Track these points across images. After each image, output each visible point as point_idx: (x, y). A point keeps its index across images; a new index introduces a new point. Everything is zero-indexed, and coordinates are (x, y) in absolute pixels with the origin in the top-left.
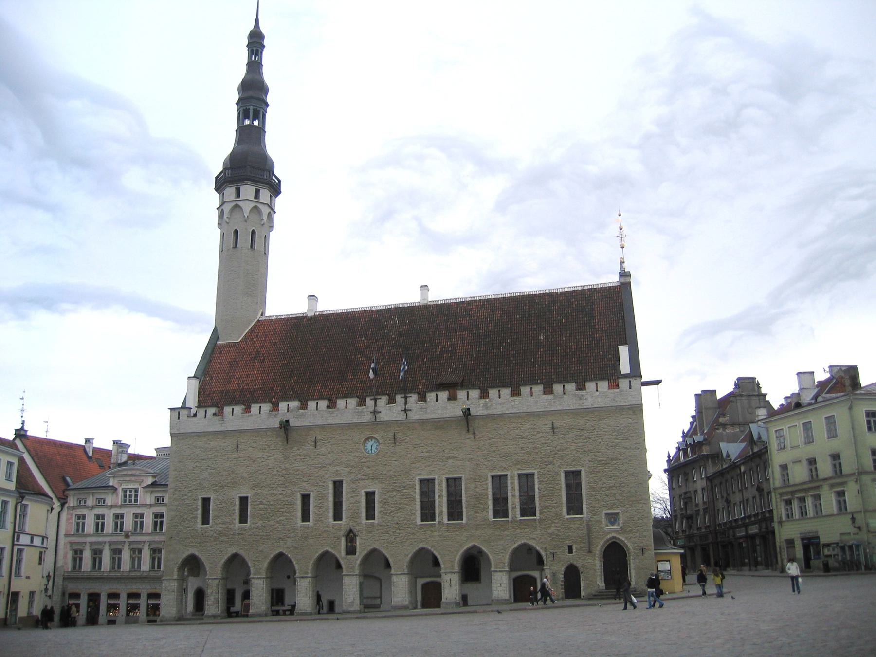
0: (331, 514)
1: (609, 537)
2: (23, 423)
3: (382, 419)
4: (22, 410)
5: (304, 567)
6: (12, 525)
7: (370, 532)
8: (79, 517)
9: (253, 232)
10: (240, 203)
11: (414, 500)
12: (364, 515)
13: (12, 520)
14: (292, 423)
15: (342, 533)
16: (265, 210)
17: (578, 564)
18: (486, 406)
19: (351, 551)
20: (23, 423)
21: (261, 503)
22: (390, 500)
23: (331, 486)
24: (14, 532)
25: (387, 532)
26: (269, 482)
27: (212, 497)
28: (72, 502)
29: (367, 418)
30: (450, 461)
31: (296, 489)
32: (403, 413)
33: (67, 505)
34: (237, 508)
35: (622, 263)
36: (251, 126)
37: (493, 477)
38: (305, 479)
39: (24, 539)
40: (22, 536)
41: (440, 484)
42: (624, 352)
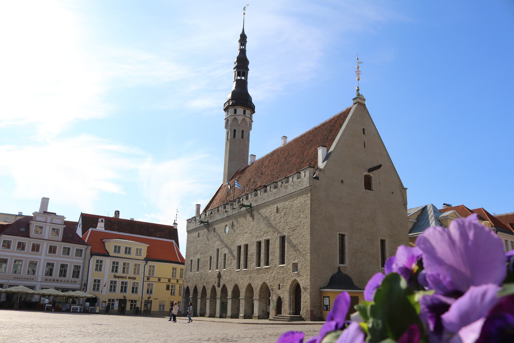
1: (293, 279)
3: (229, 215)
5: (209, 292)
9: (235, 131)
10: (229, 118)
14: (210, 222)
16: (240, 119)
17: (281, 297)
18: (256, 201)
19: (219, 286)
23: (216, 251)
29: (226, 215)
35: (358, 90)
36: (241, 80)
37: (257, 242)
40: (150, 278)
42: (321, 152)
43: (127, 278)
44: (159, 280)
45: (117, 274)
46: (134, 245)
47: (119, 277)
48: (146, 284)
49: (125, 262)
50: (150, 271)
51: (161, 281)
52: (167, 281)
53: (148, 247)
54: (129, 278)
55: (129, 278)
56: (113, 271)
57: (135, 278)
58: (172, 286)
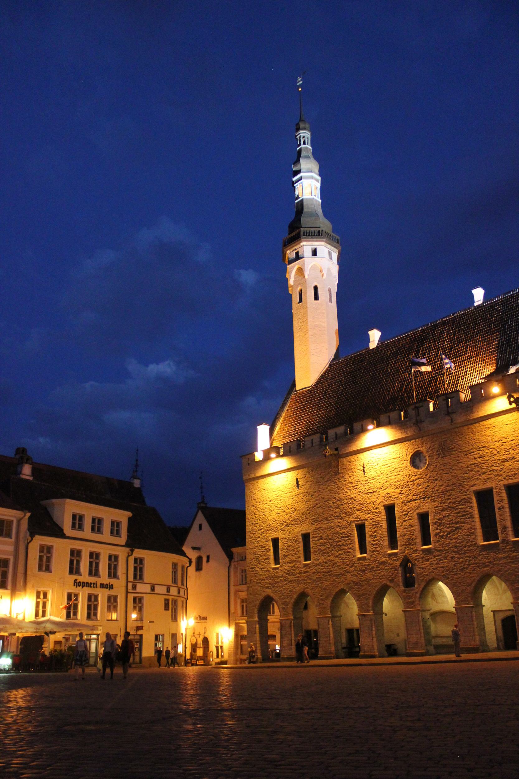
0: (386, 543)
2: (203, 498)
4: (202, 488)
6: (124, 576)
7: (428, 560)
8: (242, 571)
9: (316, 288)
11: (472, 517)
12: (419, 540)
13: (125, 572)
15: (399, 562)
20: (203, 498)
21: (321, 538)
22: (445, 521)
24: (127, 582)
25: (445, 558)
26: (326, 515)
27: (280, 535)
28: (235, 557)
30: (507, 464)
31: (351, 519)
32: (447, 418)
33: (233, 560)
34: (301, 545)
38: (358, 508)
39: (140, 587)
40: (139, 586)
41: (499, 494)
43: (98, 585)
44: (153, 589)
45: (80, 579)
46: (109, 515)
47: (84, 585)
48: (131, 597)
49: (93, 550)
50: (135, 568)
51: (156, 591)
52: (163, 590)
53: (130, 519)
54: (102, 586)
55: (102, 586)
56: (71, 572)
57: (111, 587)
58: (172, 600)
